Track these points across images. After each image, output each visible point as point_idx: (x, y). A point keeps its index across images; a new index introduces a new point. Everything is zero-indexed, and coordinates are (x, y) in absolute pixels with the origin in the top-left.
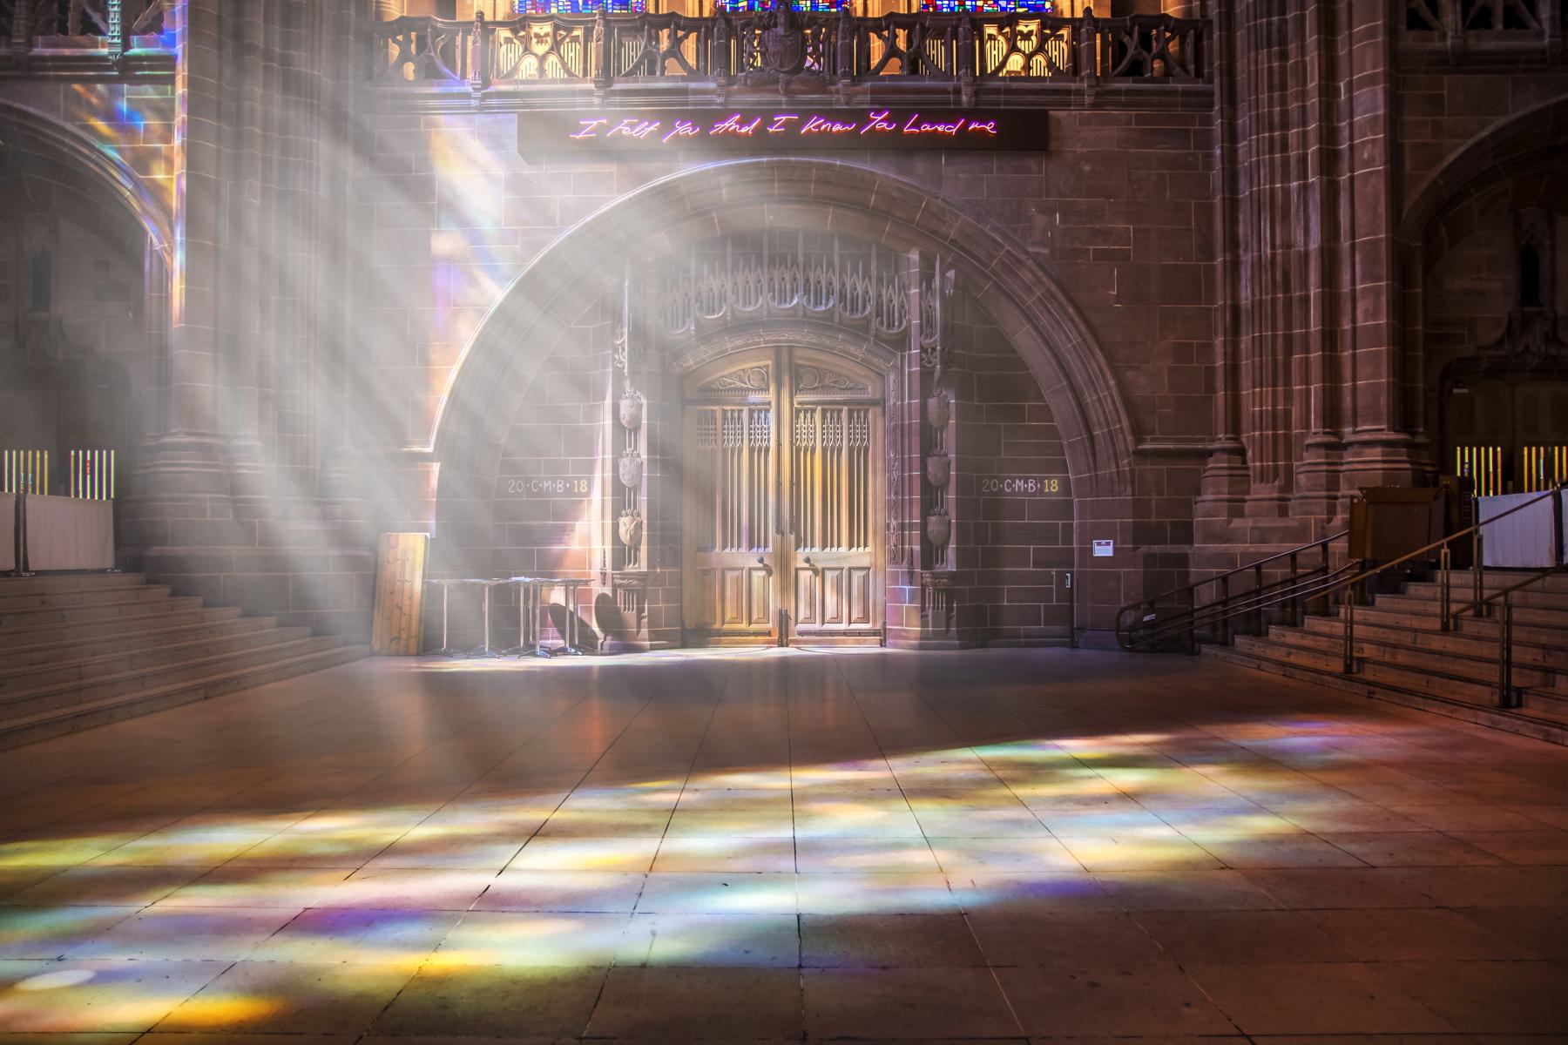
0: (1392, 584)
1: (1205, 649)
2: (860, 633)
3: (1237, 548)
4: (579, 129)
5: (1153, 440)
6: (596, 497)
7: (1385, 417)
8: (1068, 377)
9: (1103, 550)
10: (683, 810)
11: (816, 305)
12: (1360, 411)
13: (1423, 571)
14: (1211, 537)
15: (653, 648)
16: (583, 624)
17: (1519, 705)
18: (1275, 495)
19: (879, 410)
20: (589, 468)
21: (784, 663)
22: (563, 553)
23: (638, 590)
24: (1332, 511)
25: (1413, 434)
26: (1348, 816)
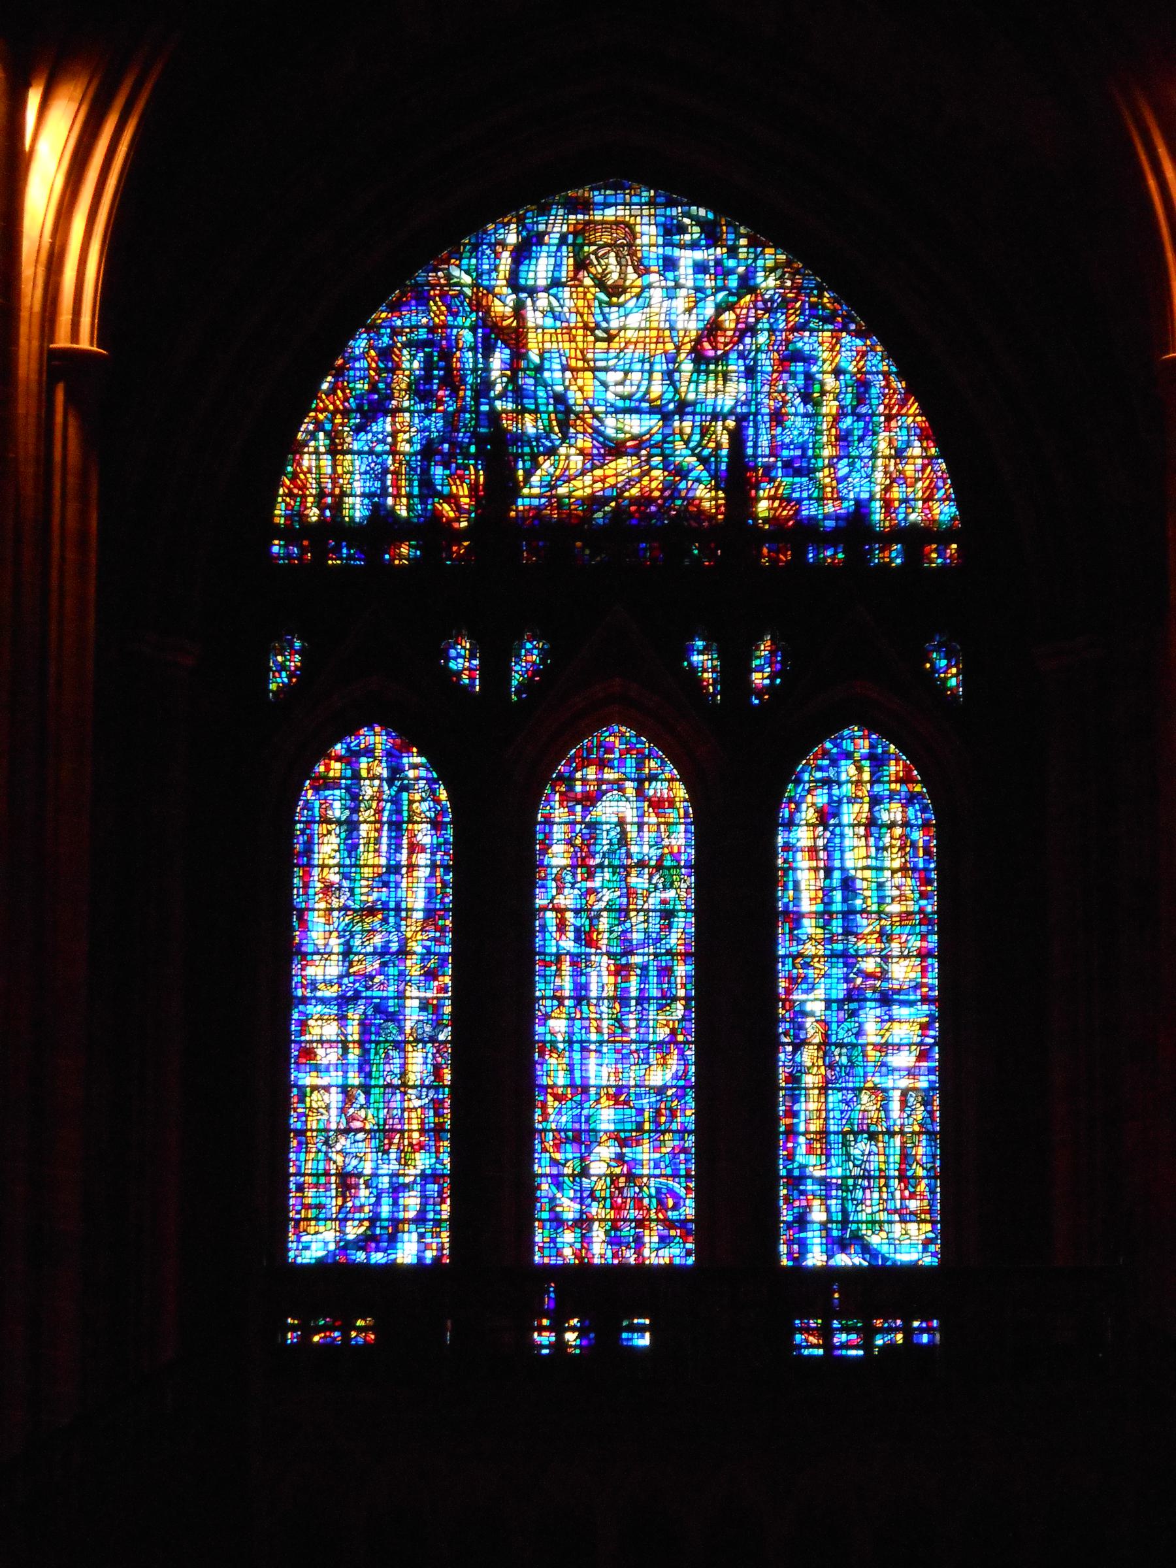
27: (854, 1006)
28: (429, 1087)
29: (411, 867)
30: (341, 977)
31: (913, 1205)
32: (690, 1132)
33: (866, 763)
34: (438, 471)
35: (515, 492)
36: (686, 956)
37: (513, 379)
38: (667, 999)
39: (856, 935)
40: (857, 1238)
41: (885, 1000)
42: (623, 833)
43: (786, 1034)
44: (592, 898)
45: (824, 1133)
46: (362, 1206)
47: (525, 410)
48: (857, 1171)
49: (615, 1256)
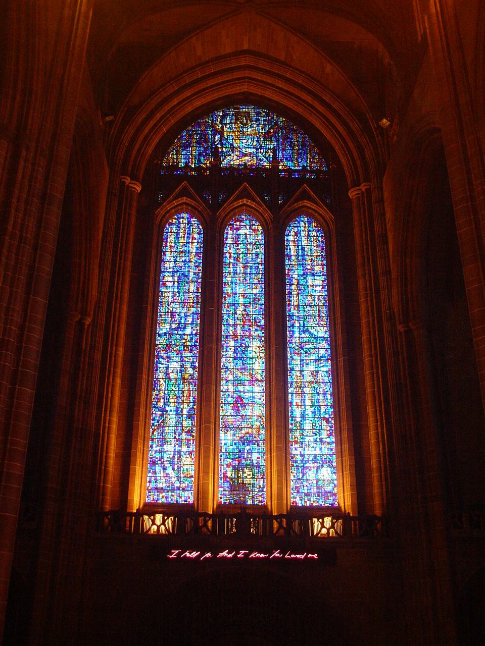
27: (305, 276)
28: (195, 292)
29: (192, 243)
30: (173, 267)
31: (322, 323)
32: (263, 304)
33: (307, 223)
36: (262, 264)
37: (221, 141)
38: (257, 274)
39: (305, 260)
40: (307, 330)
41: (313, 275)
42: (246, 236)
43: (288, 282)
44: (238, 251)
45: (298, 305)
46: (176, 321)
47: (223, 147)
48: (307, 314)
49: (243, 333)
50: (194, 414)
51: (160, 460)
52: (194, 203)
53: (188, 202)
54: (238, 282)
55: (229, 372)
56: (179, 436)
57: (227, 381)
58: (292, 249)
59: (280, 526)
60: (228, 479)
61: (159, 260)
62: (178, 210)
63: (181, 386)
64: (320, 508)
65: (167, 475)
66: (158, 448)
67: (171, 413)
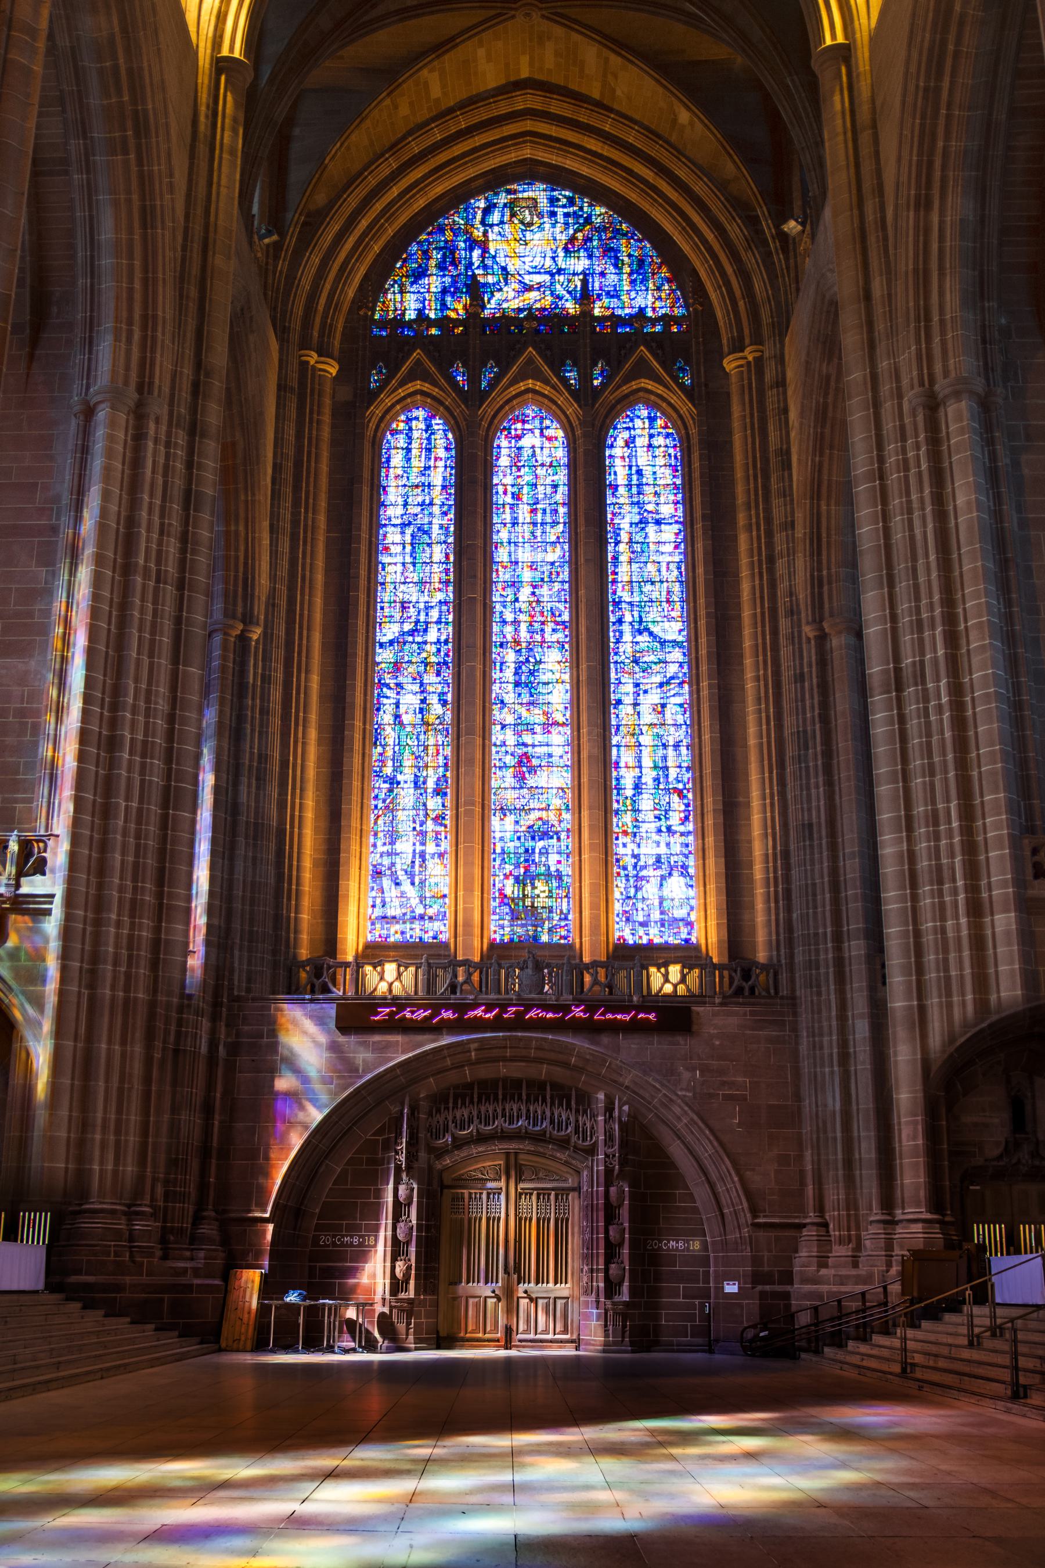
0: (933, 1314)
1: (803, 1355)
2: (561, 1341)
3: (824, 1288)
4: (378, 1014)
5: (764, 1216)
6: (380, 1247)
7: (923, 1204)
8: (705, 1174)
9: (731, 1288)
10: (434, 1460)
11: (534, 1126)
12: (906, 1200)
13: (954, 1305)
14: (805, 1281)
15: (417, 1349)
16: (368, 1332)
17: (1025, 1397)
18: (850, 1254)
19: (576, 1194)
20: (376, 1229)
21: (508, 1361)
22: (357, 1285)
23: (409, 1309)
24: (889, 1265)
25: (944, 1215)
26: (909, 1472)
29: (435, 467)
31: (673, 614)
33: (646, 421)
34: (449, 299)
35: (484, 307)
36: (564, 504)
37: (483, 262)
38: (555, 523)
40: (647, 629)
41: (658, 522)
44: (519, 480)
46: (410, 618)
47: (488, 274)
48: (646, 599)
49: (531, 638)
50: (447, 787)
51: (389, 869)
52: (435, 391)
53: (425, 389)
54: (521, 540)
55: (506, 709)
56: (421, 826)
57: (503, 727)
58: (619, 473)
59: (595, 982)
60: (506, 901)
61: (377, 504)
62: (406, 404)
63: (422, 737)
64: (666, 947)
65: (403, 894)
66: (385, 849)
67: (406, 786)
